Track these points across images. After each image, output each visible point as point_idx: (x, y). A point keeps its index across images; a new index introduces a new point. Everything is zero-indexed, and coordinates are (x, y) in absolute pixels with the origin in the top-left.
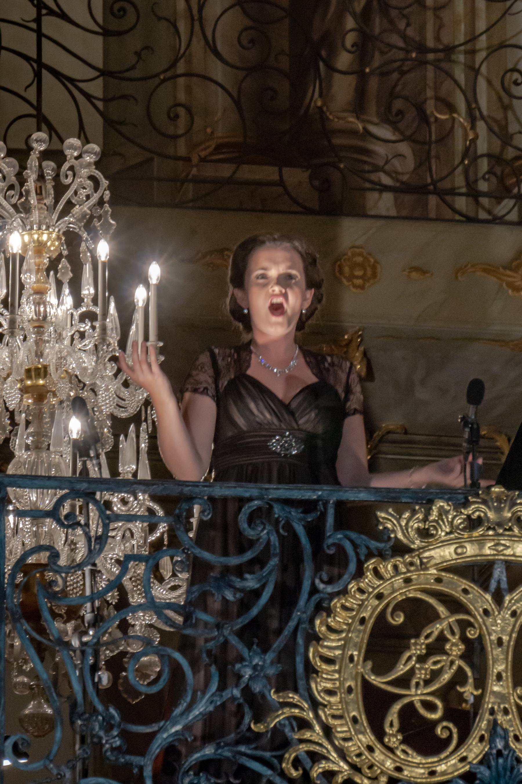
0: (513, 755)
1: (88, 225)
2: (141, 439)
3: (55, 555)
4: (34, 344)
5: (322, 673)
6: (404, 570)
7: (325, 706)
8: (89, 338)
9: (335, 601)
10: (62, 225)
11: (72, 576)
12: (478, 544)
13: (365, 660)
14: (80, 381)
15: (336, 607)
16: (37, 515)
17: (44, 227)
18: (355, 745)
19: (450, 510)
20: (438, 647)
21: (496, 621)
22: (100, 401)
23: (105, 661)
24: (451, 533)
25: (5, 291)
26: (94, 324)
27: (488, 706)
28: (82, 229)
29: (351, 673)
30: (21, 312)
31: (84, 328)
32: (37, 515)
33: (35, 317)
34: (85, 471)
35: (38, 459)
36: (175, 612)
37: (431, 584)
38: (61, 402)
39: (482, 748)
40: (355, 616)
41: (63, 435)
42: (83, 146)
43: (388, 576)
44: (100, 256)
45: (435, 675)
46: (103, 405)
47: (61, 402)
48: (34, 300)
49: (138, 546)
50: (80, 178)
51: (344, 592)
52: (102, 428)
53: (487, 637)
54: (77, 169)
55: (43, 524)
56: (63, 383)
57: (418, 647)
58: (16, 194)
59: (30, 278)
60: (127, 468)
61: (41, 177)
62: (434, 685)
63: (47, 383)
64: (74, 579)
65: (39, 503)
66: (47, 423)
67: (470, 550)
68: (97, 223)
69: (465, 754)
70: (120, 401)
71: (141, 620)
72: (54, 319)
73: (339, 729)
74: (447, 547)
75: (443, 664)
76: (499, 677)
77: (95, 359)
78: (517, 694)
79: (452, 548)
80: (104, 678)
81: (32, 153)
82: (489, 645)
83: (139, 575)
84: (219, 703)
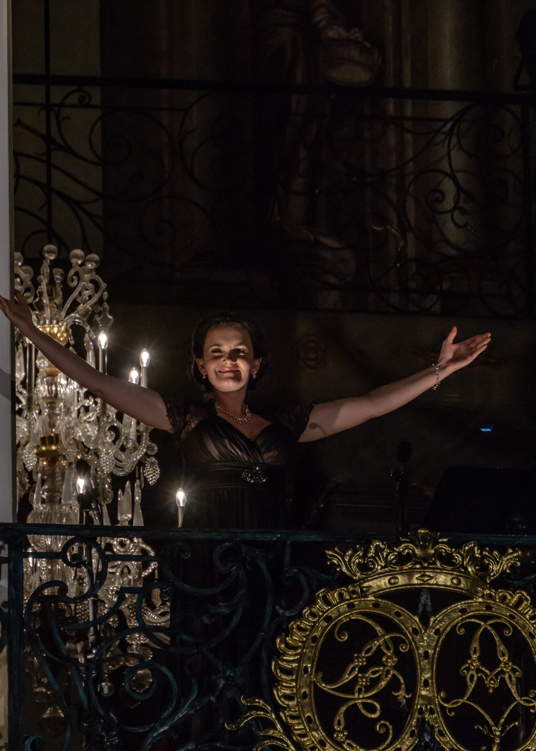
0: (438, 746)
1: (91, 321)
2: (136, 494)
3: (64, 589)
4: (47, 417)
5: (282, 682)
6: (348, 597)
7: (285, 709)
8: (92, 411)
9: (292, 623)
10: (69, 320)
11: (80, 605)
12: (408, 575)
13: (316, 672)
14: (85, 447)
15: (293, 628)
16: (51, 556)
17: (55, 322)
18: (310, 740)
19: (384, 548)
20: (376, 660)
21: (423, 638)
22: (102, 462)
23: (108, 675)
24: (386, 567)
25: (24, 374)
26: (96, 400)
27: (417, 707)
28: (86, 323)
29: (306, 681)
30: (37, 391)
31: (88, 403)
32: (51, 556)
33: (48, 395)
34: (90, 519)
35: (52, 510)
36: (165, 633)
37: (370, 609)
38: (70, 464)
39: (412, 741)
40: (308, 635)
41: (72, 491)
42: (86, 254)
43: (335, 602)
44: (101, 345)
45: (375, 682)
46: (104, 466)
47: (70, 464)
48: (47, 381)
49: (134, 580)
50: (84, 281)
51: (300, 616)
52: (104, 485)
53: (416, 651)
54: (81, 274)
55: (57, 563)
56: (72, 449)
57: (360, 660)
58: (32, 295)
59: (44, 363)
60: (124, 517)
61: (52, 282)
62: (374, 690)
63: (58, 448)
64: (82, 607)
65: (53, 546)
66: (59, 481)
67: (401, 580)
68: (98, 319)
69: (399, 746)
70: (118, 462)
71: (137, 640)
72: (63, 397)
73: (296, 727)
74: (383, 578)
75: (380, 673)
76: (426, 683)
77: (97, 429)
78: (441, 697)
79: (387, 580)
80: (105, 687)
81: (44, 262)
82: (417, 657)
83: (135, 603)
84: (198, 708)
